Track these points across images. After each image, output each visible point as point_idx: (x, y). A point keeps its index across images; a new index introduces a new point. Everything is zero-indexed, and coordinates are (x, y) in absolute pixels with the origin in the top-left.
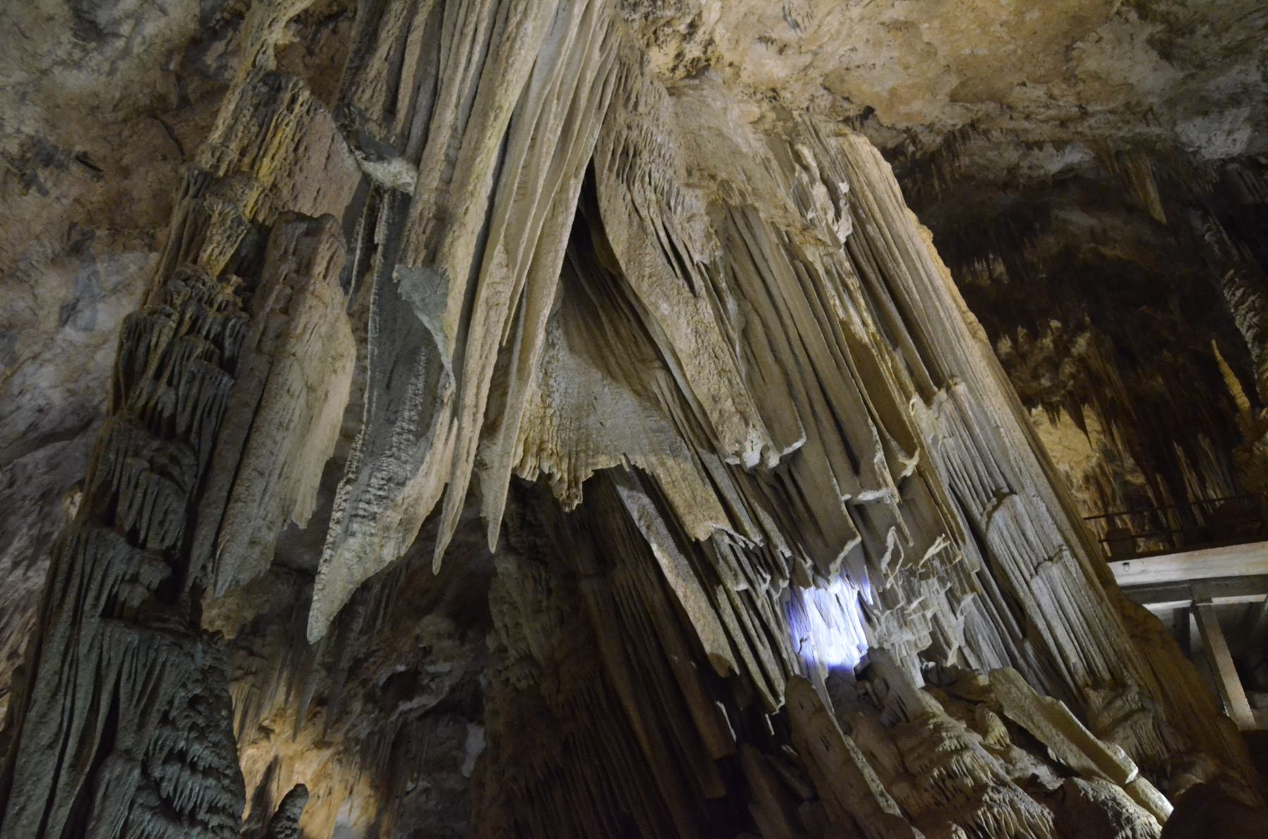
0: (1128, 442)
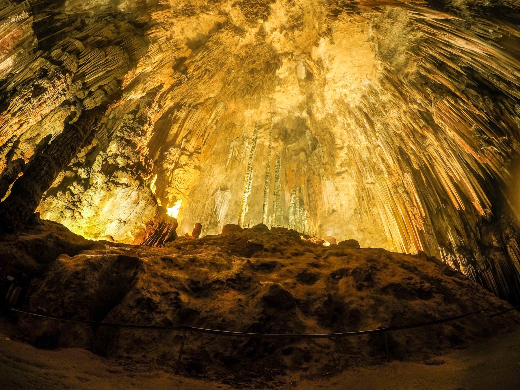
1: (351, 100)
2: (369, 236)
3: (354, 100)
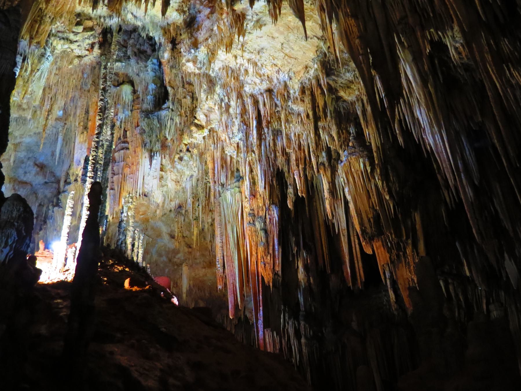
0: (346, 36)
1: (249, 81)
2: (186, 250)
3: (254, 85)
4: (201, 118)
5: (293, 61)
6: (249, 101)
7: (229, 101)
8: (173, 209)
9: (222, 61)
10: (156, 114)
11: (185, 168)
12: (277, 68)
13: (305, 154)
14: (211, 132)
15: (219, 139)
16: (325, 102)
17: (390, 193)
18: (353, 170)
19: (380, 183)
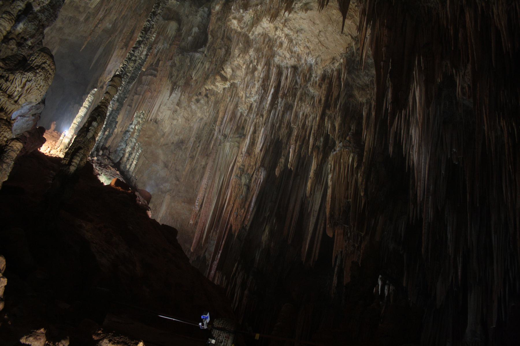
0: (376, 43)
1: (281, 54)
2: (174, 182)
3: (284, 58)
4: (228, 71)
5: (324, 49)
6: (274, 70)
7: (257, 65)
8: (175, 142)
9: (264, 28)
10: (191, 53)
11: (199, 110)
12: (308, 51)
13: (305, 134)
14: (232, 87)
15: (237, 94)
16: (339, 95)
17: (366, 190)
18: (342, 160)
19: (360, 180)
